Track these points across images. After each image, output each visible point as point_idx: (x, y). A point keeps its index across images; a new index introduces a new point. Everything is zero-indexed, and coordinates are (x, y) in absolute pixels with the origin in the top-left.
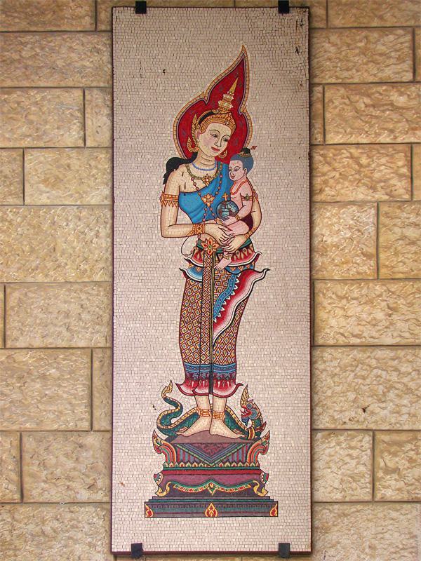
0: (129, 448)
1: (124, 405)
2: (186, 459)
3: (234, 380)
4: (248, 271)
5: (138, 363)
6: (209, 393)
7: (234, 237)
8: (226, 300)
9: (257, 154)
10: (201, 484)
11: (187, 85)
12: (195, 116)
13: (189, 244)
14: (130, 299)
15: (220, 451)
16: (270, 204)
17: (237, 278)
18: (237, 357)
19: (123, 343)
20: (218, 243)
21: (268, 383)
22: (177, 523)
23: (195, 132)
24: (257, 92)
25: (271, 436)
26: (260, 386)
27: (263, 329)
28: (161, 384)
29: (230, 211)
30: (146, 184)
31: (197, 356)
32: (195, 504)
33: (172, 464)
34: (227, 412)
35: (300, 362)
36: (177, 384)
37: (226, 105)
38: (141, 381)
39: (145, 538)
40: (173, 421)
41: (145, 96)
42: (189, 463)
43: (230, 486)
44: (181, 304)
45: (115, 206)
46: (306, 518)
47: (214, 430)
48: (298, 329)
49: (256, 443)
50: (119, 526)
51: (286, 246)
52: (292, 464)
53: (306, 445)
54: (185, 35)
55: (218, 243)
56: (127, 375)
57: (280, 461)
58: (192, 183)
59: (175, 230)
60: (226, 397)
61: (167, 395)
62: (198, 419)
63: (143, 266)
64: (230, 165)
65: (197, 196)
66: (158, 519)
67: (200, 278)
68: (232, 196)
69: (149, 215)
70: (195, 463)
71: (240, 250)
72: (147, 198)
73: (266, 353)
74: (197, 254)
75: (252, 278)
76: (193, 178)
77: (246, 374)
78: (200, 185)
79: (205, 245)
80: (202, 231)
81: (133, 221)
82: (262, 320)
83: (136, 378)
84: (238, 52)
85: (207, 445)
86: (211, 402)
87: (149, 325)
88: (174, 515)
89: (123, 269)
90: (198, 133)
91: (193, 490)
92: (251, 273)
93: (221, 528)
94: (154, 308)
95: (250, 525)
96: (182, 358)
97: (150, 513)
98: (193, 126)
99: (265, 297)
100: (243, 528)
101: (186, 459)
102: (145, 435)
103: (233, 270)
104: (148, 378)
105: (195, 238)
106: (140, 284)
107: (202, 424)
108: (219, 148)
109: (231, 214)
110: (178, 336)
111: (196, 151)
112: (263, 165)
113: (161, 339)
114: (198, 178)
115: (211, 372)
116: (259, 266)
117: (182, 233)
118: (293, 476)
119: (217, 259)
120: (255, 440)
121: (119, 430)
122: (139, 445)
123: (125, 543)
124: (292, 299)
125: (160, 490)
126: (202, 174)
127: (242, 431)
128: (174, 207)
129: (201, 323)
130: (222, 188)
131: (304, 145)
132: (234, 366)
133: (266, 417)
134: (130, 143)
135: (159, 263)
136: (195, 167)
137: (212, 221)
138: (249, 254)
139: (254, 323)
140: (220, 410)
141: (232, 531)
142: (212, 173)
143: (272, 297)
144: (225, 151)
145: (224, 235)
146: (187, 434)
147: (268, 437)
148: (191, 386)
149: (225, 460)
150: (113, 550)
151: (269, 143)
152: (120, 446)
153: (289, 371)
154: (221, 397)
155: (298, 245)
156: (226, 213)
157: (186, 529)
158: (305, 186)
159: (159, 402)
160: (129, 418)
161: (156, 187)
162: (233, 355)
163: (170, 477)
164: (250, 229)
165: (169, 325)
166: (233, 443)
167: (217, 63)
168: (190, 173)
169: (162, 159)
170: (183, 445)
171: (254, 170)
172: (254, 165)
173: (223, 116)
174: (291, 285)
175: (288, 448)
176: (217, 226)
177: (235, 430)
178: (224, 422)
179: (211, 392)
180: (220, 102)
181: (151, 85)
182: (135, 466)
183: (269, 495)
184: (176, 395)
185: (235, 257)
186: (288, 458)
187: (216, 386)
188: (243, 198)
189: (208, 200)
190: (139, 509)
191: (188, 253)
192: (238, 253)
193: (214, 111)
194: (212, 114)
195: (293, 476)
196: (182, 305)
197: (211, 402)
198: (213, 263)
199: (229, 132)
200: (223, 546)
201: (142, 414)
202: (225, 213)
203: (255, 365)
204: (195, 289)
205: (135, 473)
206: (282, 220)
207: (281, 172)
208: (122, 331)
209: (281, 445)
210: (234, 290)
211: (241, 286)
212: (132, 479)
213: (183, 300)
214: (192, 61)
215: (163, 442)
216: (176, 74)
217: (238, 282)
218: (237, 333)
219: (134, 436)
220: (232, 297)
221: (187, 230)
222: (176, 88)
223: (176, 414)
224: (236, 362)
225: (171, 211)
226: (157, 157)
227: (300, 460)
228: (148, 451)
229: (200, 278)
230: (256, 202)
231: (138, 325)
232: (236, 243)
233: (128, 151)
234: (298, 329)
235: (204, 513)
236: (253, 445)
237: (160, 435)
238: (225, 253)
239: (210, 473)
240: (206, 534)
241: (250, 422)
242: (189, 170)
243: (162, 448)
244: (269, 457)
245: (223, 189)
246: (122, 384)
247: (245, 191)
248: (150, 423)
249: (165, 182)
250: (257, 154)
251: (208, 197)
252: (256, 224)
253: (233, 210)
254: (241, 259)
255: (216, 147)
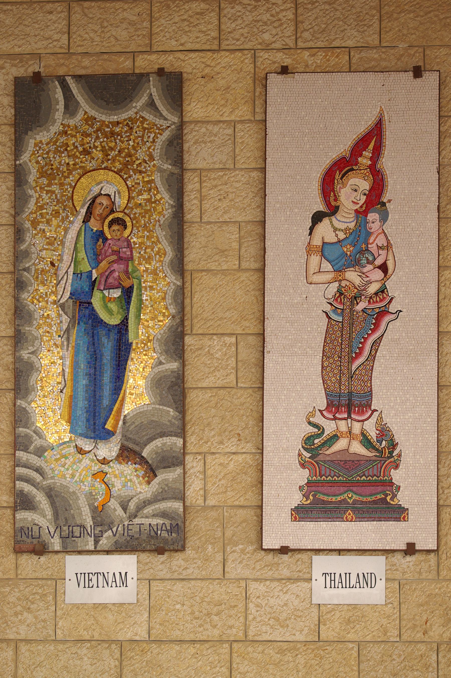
0: (278, 464)
1: (273, 428)
2: (328, 473)
3: (370, 406)
4: (383, 313)
5: (285, 392)
6: (348, 418)
7: (371, 283)
8: (363, 337)
9: (392, 207)
10: (341, 494)
11: (331, 144)
12: (338, 172)
13: (331, 289)
14: (278, 337)
15: (357, 467)
16: (403, 253)
17: (373, 318)
18: (373, 387)
19: (273, 375)
20: (356, 288)
21: (400, 409)
22: (319, 526)
23: (337, 187)
24: (392, 149)
25: (403, 454)
26: (393, 412)
27: (396, 363)
28: (306, 410)
29: (367, 259)
30: (294, 236)
31: (337, 385)
32: (335, 511)
33: (315, 477)
34: (363, 434)
35: (428, 391)
36: (319, 410)
37: (365, 161)
38: (288, 407)
39: (291, 538)
40: (316, 441)
41: (294, 154)
42: (329, 477)
43: (366, 496)
44: (323, 341)
45: (266, 256)
46: (433, 522)
47: (352, 449)
48: (427, 362)
49: (389, 460)
50: (269, 528)
51: (417, 290)
52: (421, 478)
53: (433, 462)
54: (330, 98)
55: (356, 288)
56: (276, 402)
57: (410, 475)
58: (334, 234)
59: (318, 277)
60: (363, 421)
61: (311, 419)
62: (337, 440)
63: (290, 309)
64: (368, 218)
65: (338, 246)
66: (303, 523)
67: (340, 319)
68: (369, 246)
69: (296, 264)
70: (335, 477)
71: (376, 294)
72: (295, 248)
73: (398, 383)
74: (338, 297)
75: (387, 318)
76: (335, 230)
77: (381, 401)
78: (342, 236)
79: (345, 290)
80: (342, 278)
81: (282, 269)
82: (395, 355)
83: (284, 405)
84: (376, 112)
85: (346, 461)
86: (350, 426)
87: (295, 360)
88: (316, 519)
89: (273, 311)
90: (340, 188)
91: (334, 499)
92: (385, 314)
93: (358, 531)
94: (300, 344)
95: (384, 528)
96: (325, 388)
97: (295, 517)
98: (336, 181)
99: (397, 335)
100: (378, 530)
101: (328, 473)
102: (292, 454)
103: (369, 312)
104: (294, 405)
105: (336, 284)
106: (288, 324)
107: (341, 444)
108: (358, 202)
109: (369, 262)
110: (321, 369)
111: (337, 205)
112: (397, 217)
113: (305, 372)
114: (340, 230)
115: (350, 400)
116: (392, 308)
117: (325, 280)
118: (421, 488)
119: (355, 302)
120: (389, 458)
121: (268, 449)
122: (286, 462)
123: (274, 542)
124: (422, 337)
125: (305, 499)
126: (343, 226)
127: (377, 450)
128: (318, 257)
129: (341, 358)
130: (361, 238)
131: (433, 199)
132: (370, 393)
133: (397, 439)
134: (280, 198)
135: (305, 306)
136: (337, 220)
137: (351, 269)
138: (384, 298)
139: (388, 358)
140: (357, 432)
141: (367, 533)
142: (352, 225)
143: (404, 334)
144: (363, 204)
145: (362, 281)
146: (328, 452)
147: (399, 455)
148: (332, 411)
149: (362, 474)
150: (264, 547)
151: (402, 197)
152: (270, 462)
153: (419, 399)
154: (359, 421)
155: (427, 290)
156: (364, 261)
157: (327, 531)
158: (434, 237)
159: (304, 426)
160: (277, 438)
161: (303, 238)
162: (369, 385)
163: (313, 488)
164: (385, 276)
165: (313, 359)
166: (369, 460)
167: (357, 123)
168: (332, 225)
169: (308, 213)
170: (324, 462)
171: (389, 222)
172: (390, 218)
173: (362, 171)
174: (421, 324)
175: (417, 465)
176: (356, 273)
177: (370, 449)
178: (361, 442)
179: (349, 417)
180: (360, 159)
181: (299, 144)
182: (282, 480)
183: (400, 503)
184: (318, 419)
185: (371, 300)
186: (418, 473)
187: (354, 412)
188: (379, 248)
189: (349, 250)
190: (286, 514)
191: (330, 297)
192: (374, 297)
193: (354, 167)
194: (352, 170)
195: (421, 488)
196: (325, 342)
197: (350, 426)
198: (352, 304)
199: (368, 188)
200: (360, 545)
201: (289, 436)
202: (363, 261)
203: (389, 393)
204: (336, 328)
205: (283, 485)
206: (414, 268)
207: (414, 224)
208: (271, 365)
209: (411, 462)
210: (370, 329)
211: (377, 326)
212: (280, 490)
213: (325, 337)
214: (335, 121)
215: (307, 459)
216: (321, 133)
217: (374, 321)
218: (373, 366)
219: (282, 454)
220: (369, 335)
221: (330, 276)
222: (321, 146)
223: (318, 436)
224: (371, 391)
225: (315, 259)
226: (304, 210)
227: (428, 475)
228: (294, 467)
229: (340, 319)
230: (391, 251)
231: (285, 360)
232: (373, 288)
233: (278, 206)
234: (427, 362)
235: (343, 518)
236: (386, 463)
237: (305, 453)
238: (363, 297)
239: (348, 485)
240: (345, 535)
241: (384, 442)
242: (331, 222)
243: (307, 465)
244: (401, 472)
245: (362, 239)
246: (271, 410)
247: (381, 241)
248: (296, 443)
249: (310, 234)
250: (392, 207)
251: (348, 247)
252: (390, 271)
253: (371, 258)
254: (377, 302)
255: (355, 201)
